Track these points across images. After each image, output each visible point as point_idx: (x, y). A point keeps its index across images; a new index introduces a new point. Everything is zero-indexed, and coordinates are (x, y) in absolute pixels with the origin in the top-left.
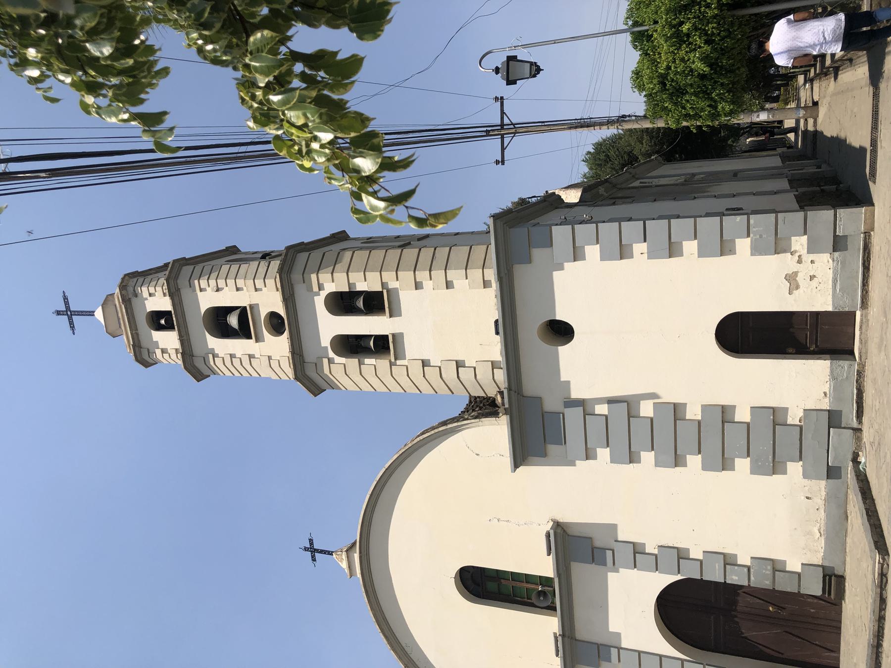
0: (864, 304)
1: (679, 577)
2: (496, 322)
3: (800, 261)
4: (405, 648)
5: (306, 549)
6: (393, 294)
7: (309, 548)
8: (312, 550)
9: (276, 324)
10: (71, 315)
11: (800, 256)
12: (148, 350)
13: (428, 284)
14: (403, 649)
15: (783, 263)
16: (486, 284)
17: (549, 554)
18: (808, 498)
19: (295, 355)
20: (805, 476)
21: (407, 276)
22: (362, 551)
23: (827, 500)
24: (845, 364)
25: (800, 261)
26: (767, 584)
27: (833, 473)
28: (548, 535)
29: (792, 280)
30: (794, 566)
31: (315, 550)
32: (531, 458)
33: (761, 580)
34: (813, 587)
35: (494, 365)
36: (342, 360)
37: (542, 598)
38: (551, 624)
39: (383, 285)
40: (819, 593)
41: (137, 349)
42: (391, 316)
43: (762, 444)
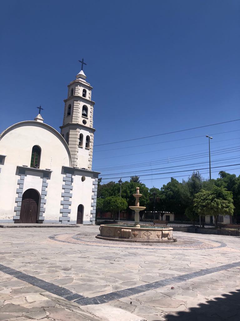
0: (84, 225)
1: (41, 195)
2: (85, 169)
5: (40, 107)
6: (89, 149)
9: (84, 122)
13: (89, 157)
15: (89, 214)
16: (89, 168)
17: (46, 169)
21: (92, 154)
23: (56, 220)
26: (41, 210)
27: (60, 221)
28: (49, 170)
29: (87, 215)
30: (44, 215)
32: (63, 170)
33: (41, 209)
34: (40, 218)
35: (77, 166)
36: (79, 135)
38: (29, 166)
39: (90, 149)
40: (40, 219)
42: (85, 148)
43: (65, 210)
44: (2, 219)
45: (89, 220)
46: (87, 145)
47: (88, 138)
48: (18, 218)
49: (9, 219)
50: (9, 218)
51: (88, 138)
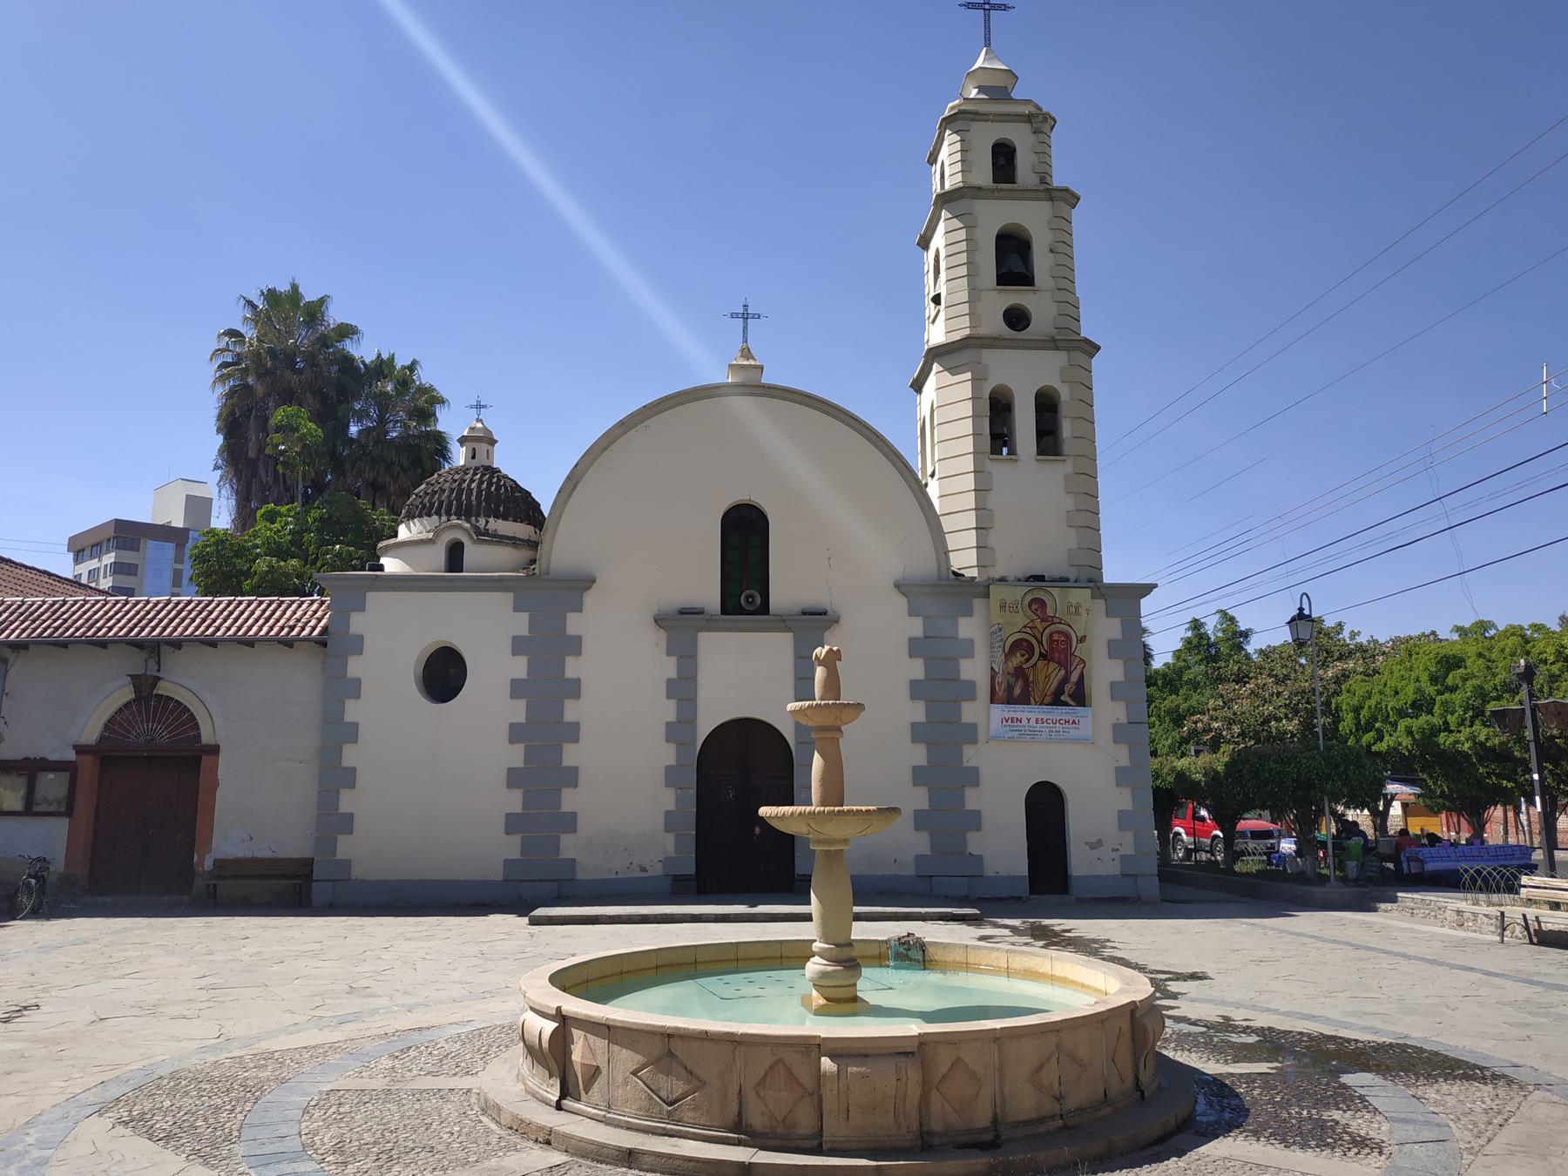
3: (1113, 850)
4: (644, 424)
7: (746, 310)
8: (745, 317)
10: (985, 9)
11: (1118, 850)
12: (968, 131)
14: (642, 421)
18: (895, 860)
19: (992, 340)
20: (918, 858)
22: (770, 390)
24: (1027, 887)
25: (1113, 850)
28: (825, 613)
29: (1095, 845)
31: (747, 318)
37: (750, 600)
41: (971, 116)
44: (615, 877)
45: (1112, 868)
46: (1048, 440)
47: (1047, 406)
48: (689, 868)
49: (645, 874)
50: (643, 870)
51: (1047, 406)
